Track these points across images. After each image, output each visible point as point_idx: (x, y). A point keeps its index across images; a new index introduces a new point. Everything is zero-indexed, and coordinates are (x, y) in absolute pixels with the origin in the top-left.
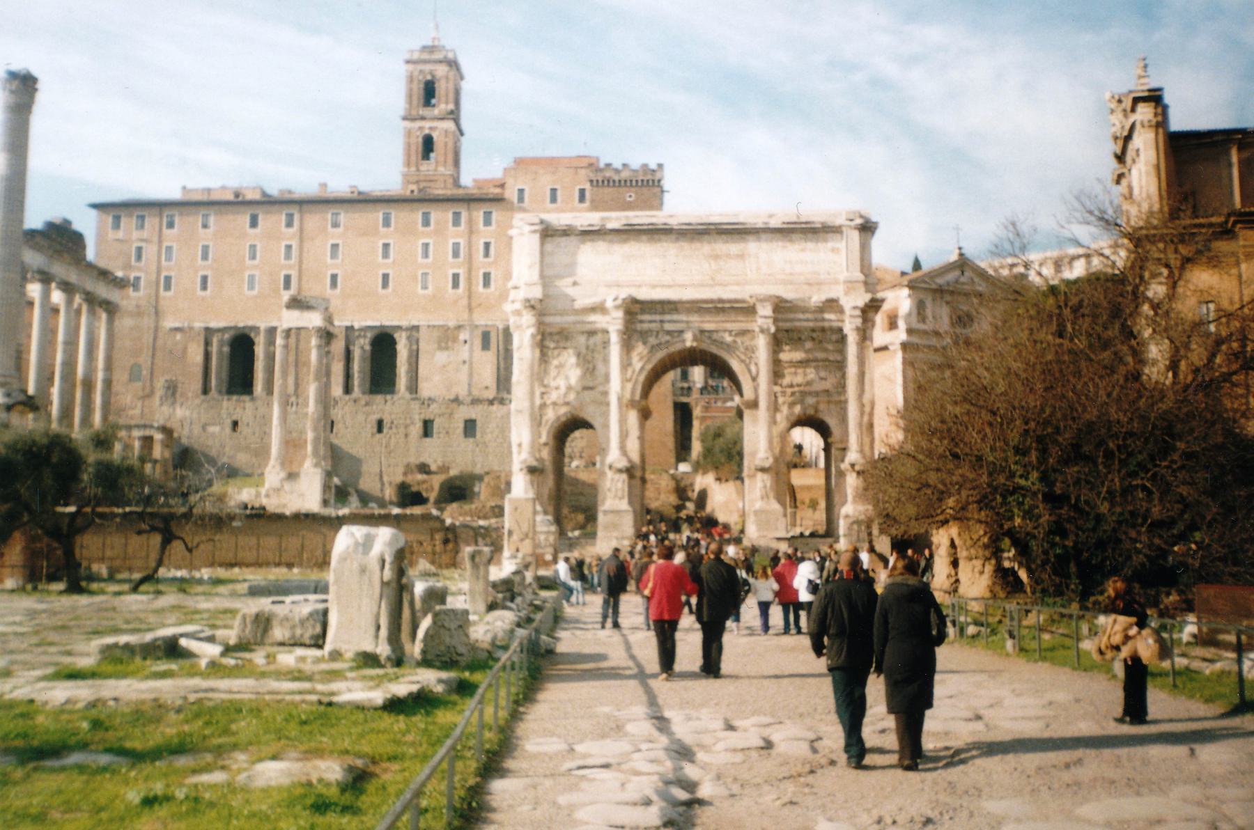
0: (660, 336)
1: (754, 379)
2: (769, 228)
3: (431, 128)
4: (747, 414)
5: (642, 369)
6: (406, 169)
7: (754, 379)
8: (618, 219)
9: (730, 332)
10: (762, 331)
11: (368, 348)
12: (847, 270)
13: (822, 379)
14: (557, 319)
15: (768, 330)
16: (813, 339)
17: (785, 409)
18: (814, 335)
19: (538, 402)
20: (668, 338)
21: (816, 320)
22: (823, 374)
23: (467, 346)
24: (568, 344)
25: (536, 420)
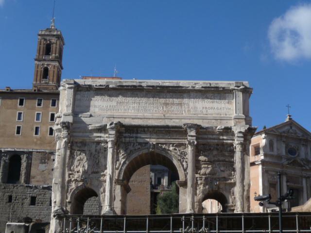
0: (135, 145)
1: (185, 170)
2: (195, 90)
3: (48, 65)
4: (181, 190)
5: (124, 163)
6: (35, 82)
7: (185, 170)
8: (115, 83)
9: (174, 144)
10: (190, 143)
11: (7, 161)
12: (236, 113)
13: (222, 171)
14: (81, 134)
15: (193, 142)
16: (217, 149)
17: (201, 187)
18: (218, 147)
19: (67, 179)
20: (139, 146)
22: (222, 169)
24: (86, 148)
25: (64, 189)
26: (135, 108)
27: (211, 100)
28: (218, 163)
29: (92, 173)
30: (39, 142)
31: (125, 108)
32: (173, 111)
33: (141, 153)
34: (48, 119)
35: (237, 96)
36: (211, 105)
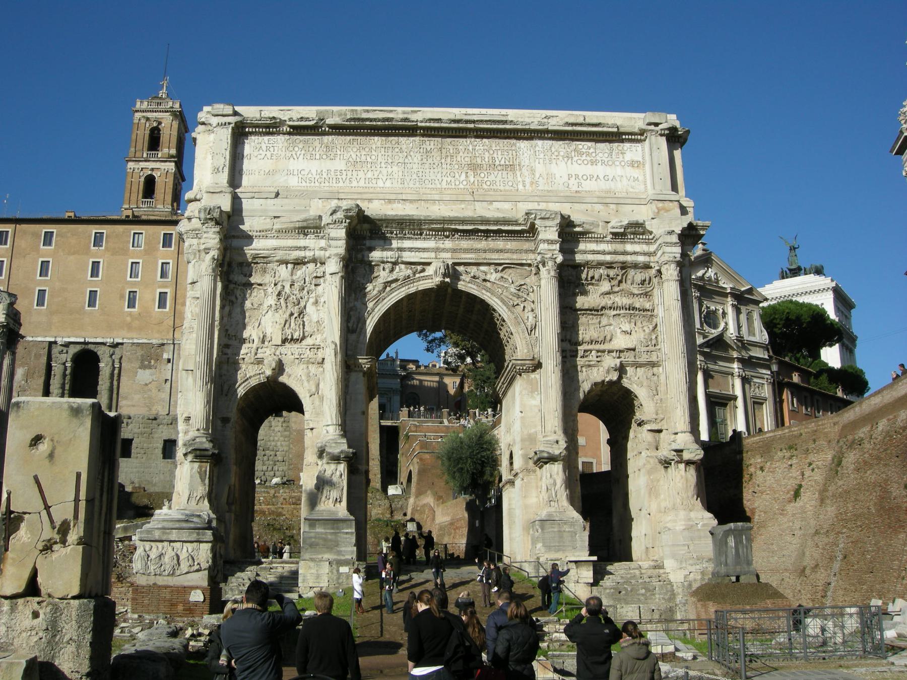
2: (547, 131)
3: (152, 170)
8: (340, 115)
13: (625, 332)
18: (612, 273)
21: (615, 253)
22: (626, 327)
23: (170, 365)
26: (396, 176)
27: (589, 158)
28: (615, 312)
29: (284, 341)
30: (136, 323)
31: (369, 175)
32: (493, 183)
33: (412, 289)
34: (156, 276)
35: (655, 147)
36: (589, 170)
